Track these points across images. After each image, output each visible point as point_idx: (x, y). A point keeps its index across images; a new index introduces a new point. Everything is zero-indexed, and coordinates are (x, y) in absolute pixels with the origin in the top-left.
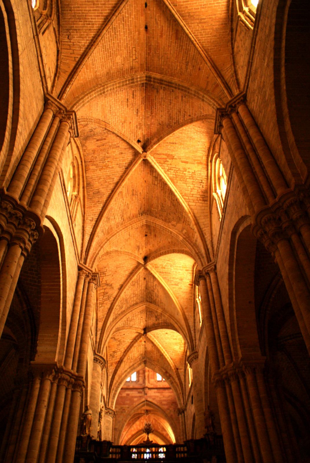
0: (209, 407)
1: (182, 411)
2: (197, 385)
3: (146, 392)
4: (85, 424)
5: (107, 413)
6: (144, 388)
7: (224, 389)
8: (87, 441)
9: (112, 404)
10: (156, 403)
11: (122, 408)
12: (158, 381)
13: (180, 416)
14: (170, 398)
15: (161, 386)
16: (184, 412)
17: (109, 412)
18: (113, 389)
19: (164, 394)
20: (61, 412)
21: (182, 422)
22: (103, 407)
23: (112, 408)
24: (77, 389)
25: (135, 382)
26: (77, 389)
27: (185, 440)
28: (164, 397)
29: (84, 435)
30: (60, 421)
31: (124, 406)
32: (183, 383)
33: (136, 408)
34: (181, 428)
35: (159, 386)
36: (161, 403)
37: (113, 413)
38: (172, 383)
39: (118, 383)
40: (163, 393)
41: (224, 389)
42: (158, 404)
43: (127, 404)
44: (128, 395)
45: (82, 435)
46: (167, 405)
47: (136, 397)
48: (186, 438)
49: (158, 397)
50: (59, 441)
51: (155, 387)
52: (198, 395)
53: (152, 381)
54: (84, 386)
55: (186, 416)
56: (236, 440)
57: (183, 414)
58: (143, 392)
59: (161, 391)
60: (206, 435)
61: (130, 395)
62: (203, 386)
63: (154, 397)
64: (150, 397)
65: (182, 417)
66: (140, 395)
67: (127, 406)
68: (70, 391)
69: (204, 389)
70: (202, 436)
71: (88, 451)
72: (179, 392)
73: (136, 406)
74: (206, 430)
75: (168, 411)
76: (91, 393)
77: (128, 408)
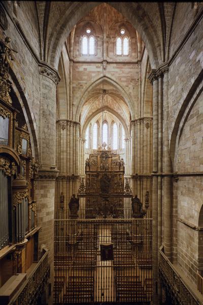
6: (102, 63)
11: (79, 83)
12: (118, 56)
19: (123, 69)
25: (93, 55)
28: (123, 73)
31: (81, 82)
33: (94, 84)
35: (118, 61)
42: (117, 81)
43: (84, 80)
44: (85, 69)
47: (94, 72)
49: (117, 72)
53: (111, 54)
59: (121, 65)
61: (88, 70)
63: (112, 73)
64: (109, 72)
66: (99, 70)
67: (84, 82)
73: (94, 82)
77: (86, 83)
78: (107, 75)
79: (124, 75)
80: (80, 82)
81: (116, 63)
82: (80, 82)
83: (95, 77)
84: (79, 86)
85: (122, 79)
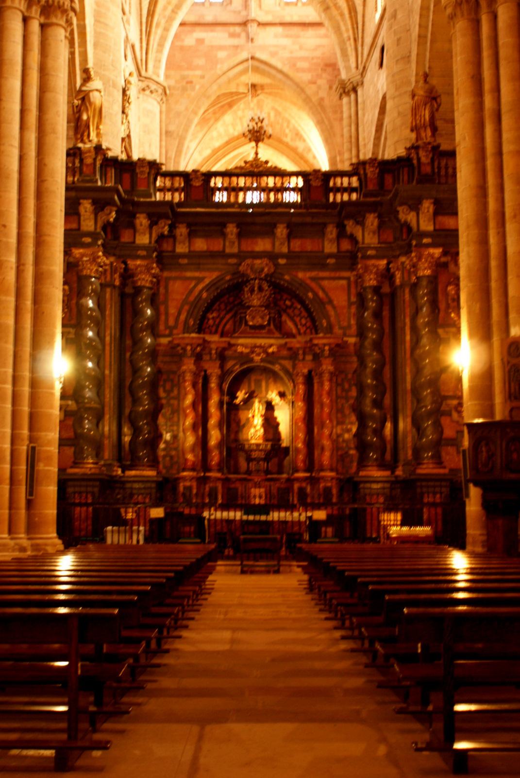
0: (426, 76)
1: (349, 87)
2: (399, 16)
3: (251, 36)
4: (85, 117)
5: (144, 90)
6: (245, 24)
7: (476, 24)
8: (95, 159)
9: (157, 67)
10: (279, 65)
11: (183, 77)
13: (345, 100)
14: (318, 53)
15: (296, 19)
16: (355, 90)
17: (148, 86)
18: (158, 25)
20: (17, 84)
21: (350, 117)
22: (130, 74)
23: (158, 76)
24: (54, 20)
26: (54, 20)
27: (354, 161)
28: (301, 48)
29: (85, 143)
30: (17, 107)
31: (190, 73)
32: (359, 9)
33: (224, 79)
34: (346, 130)
35: (288, 19)
36: (294, 65)
37: (160, 91)
38: (327, 9)
39: (170, 8)
40: (298, 37)
41: (476, 24)
42: (286, 69)
43: (197, 68)
44: (200, 41)
45: (80, 145)
46: (309, 70)
47: (221, 48)
48: (358, 156)
49: (284, 48)
50: (22, 158)
51: (277, 21)
52: (398, 45)
54: (73, 10)
55: (360, 100)
56: (490, 163)
57: (353, 96)
58: (243, 35)
59: (295, 30)
60: (414, 148)
61: (207, 42)
62: (417, 18)
64: (263, 48)
65: (350, 103)
66: (235, 41)
68: (35, 26)
69: (417, 27)
70: (401, 152)
71: (99, 183)
72: (345, 35)
73: (224, 74)
74: (413, 136)
75: (313, 88)
76: (97, 34)
77: (203, 77)
78: (258, 55)
79: (303, 54)
80: (186, 73)
81: (282, 24)
82: (186, 73)
83: (225, 60)
84: (184, 84)
85: (301, 64)
